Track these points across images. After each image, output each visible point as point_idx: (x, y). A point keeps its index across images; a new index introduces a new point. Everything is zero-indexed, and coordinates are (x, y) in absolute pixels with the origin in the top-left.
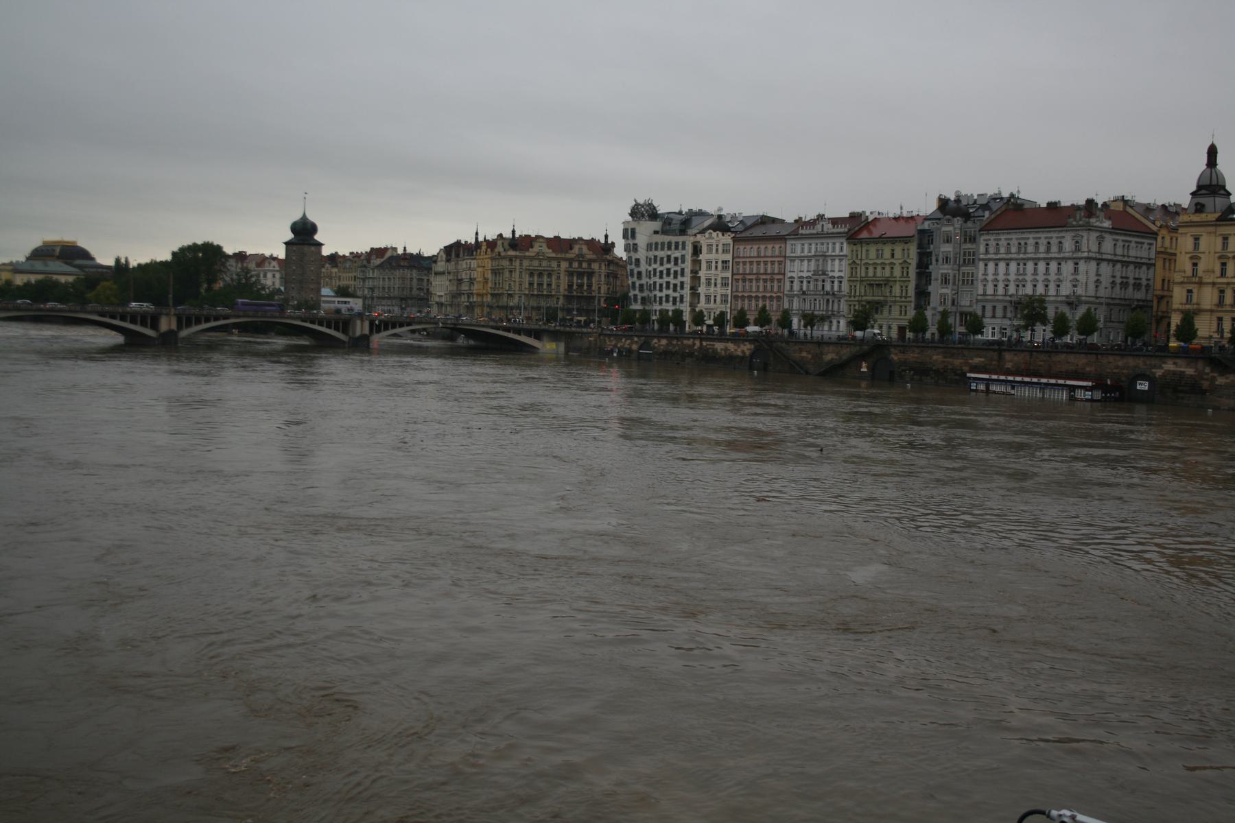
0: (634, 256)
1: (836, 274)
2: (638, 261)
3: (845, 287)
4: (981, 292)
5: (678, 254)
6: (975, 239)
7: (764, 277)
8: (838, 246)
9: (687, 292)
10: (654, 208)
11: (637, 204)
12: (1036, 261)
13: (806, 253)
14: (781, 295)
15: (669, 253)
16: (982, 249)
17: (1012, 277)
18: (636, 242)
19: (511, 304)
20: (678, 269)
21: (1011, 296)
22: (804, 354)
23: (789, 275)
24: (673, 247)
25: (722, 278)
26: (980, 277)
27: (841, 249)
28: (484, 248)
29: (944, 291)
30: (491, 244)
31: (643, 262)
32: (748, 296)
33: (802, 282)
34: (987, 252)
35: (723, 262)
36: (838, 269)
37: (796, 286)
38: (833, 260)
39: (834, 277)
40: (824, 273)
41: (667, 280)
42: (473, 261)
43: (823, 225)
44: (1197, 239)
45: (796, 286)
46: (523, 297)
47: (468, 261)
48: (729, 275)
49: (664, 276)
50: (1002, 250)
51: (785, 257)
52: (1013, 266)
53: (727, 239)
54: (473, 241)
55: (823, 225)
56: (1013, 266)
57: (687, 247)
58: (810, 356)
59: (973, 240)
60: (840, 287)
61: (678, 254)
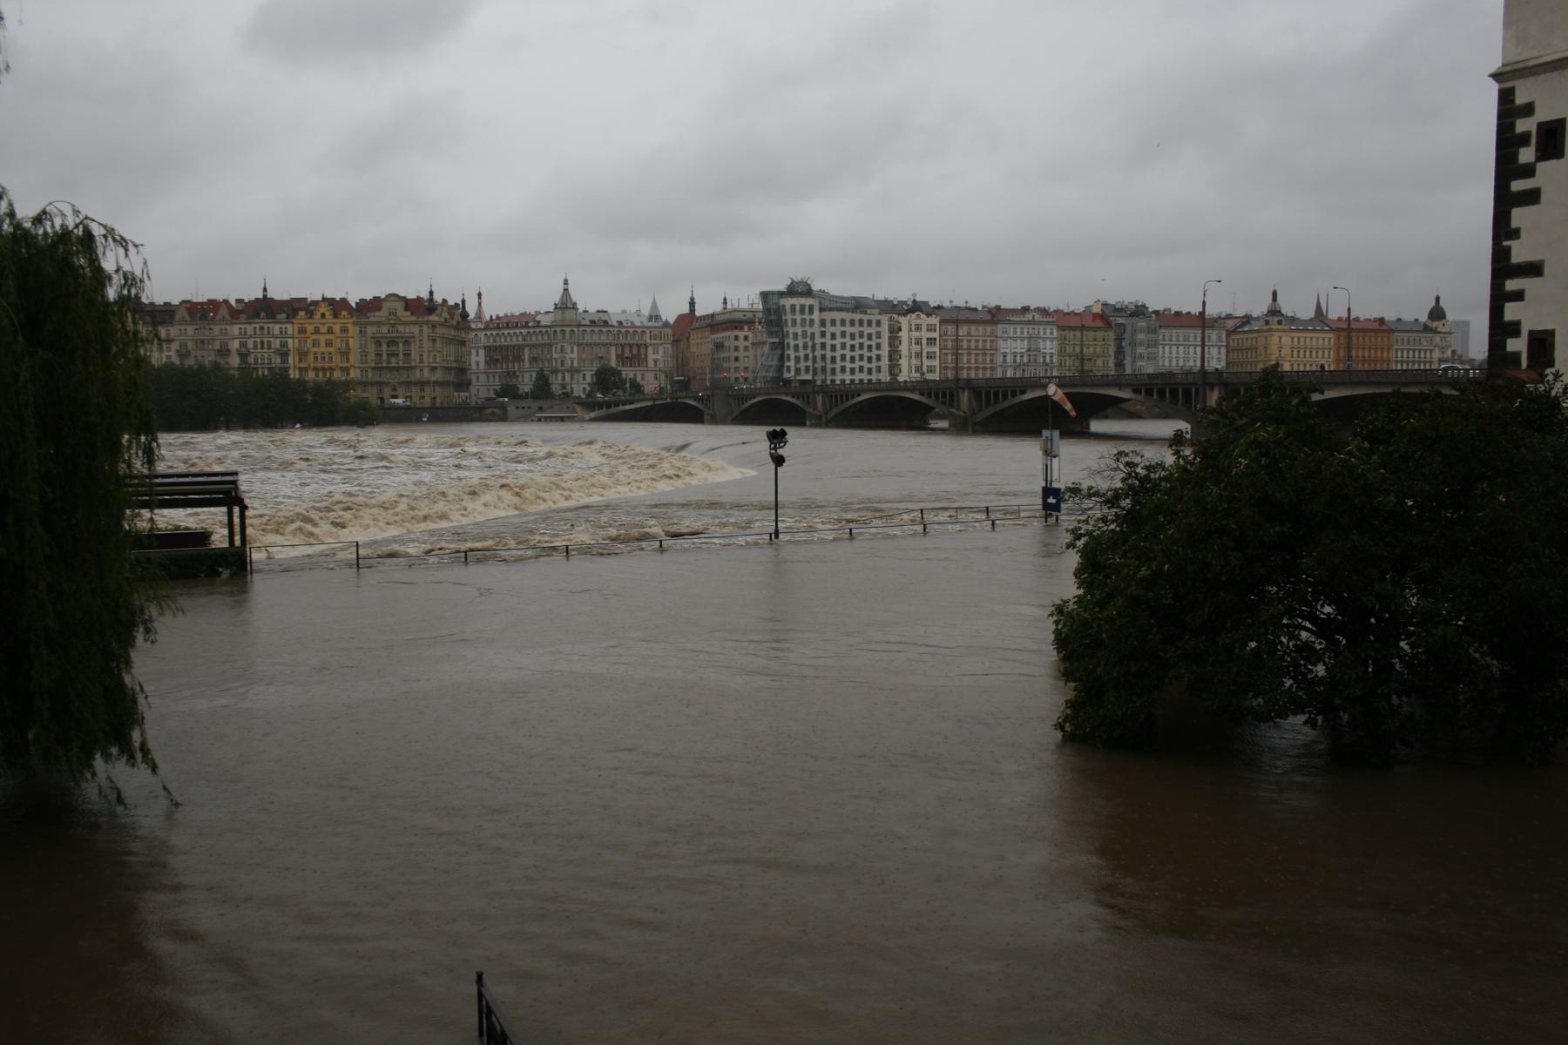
0: (809, 331)
1: (1048, 351)
2: (813, 336)
3: (1055, 359)
4: (1161, 364)
5: (872, 330)
6: (1155, 330)
7: (977, 352)
8: (1048, 331)
9: (885, 362)
10: (809, 285)
11: (793, 282)
12: (1195, 346)
13: (1019, 335)
14: (994, 366)
15: (861, 329)
16: (1161, 337)
17: (1181, 355)
18: (812, 317)
19: (433, 379)
20: (873, 343)
21: (1182, 367)
22: (1138, 407)
23: (1003, 351)
24: (865, 324)
25: (928, 352)
26: (1161, 355)
27: (1051, 333)
28: (323, 309)
29: (1141, 363)
30: (337, 306)
31: (817, 335)
32: (976, 367)
33: (1015, 356)
34: (1164, 340)
35: (928, 339)
36: (1049, 347)
37: (1009, 359)
38: (1045, 341)
39: (1046, 353)
40: (1038, 350)
41: (861, 352)
42: (276, 329)
43: (1034, 316)
44: (1280, 338)
45: (1009, 359)
46: (370, 370)
47: (271, 325)
48: (936, 349)
49: (857, 349)
50: (1174, 339)
51: (997, 337)
52: (1181, 349)
53: (935, 320)
54: (261, 296)
55: (1034, 316)
56: (1181, 349)
57: (882, 325)
58: (1143, 408)
59: (1154, 332)
60: (1051, 361)
61: (872, 330)
